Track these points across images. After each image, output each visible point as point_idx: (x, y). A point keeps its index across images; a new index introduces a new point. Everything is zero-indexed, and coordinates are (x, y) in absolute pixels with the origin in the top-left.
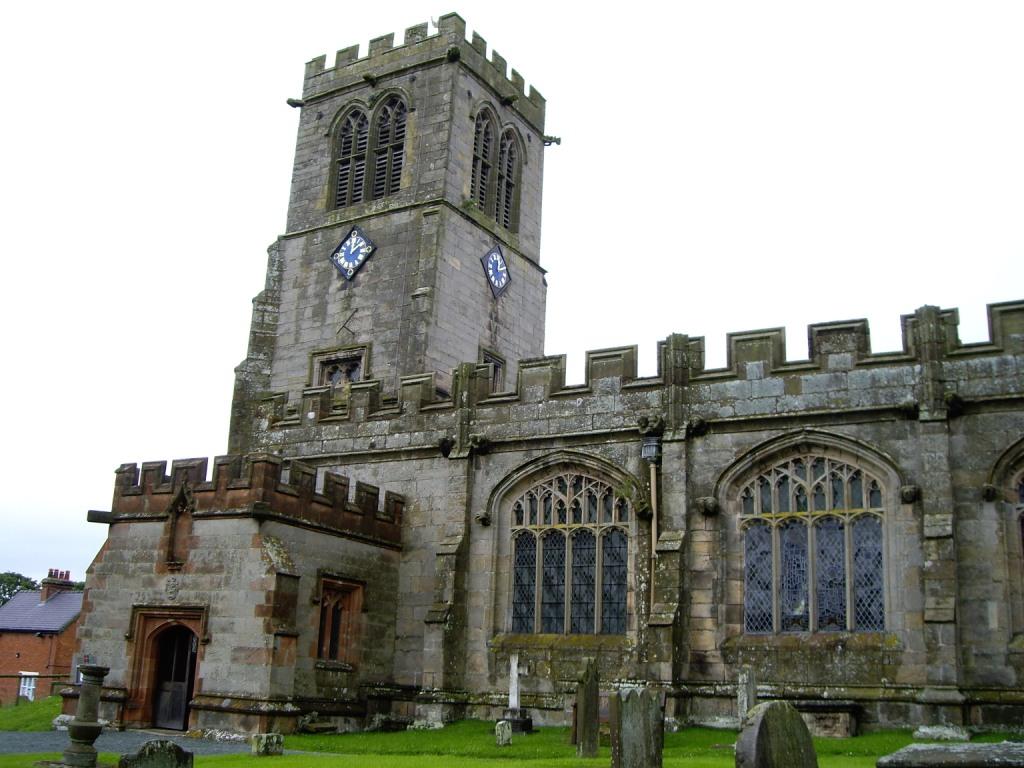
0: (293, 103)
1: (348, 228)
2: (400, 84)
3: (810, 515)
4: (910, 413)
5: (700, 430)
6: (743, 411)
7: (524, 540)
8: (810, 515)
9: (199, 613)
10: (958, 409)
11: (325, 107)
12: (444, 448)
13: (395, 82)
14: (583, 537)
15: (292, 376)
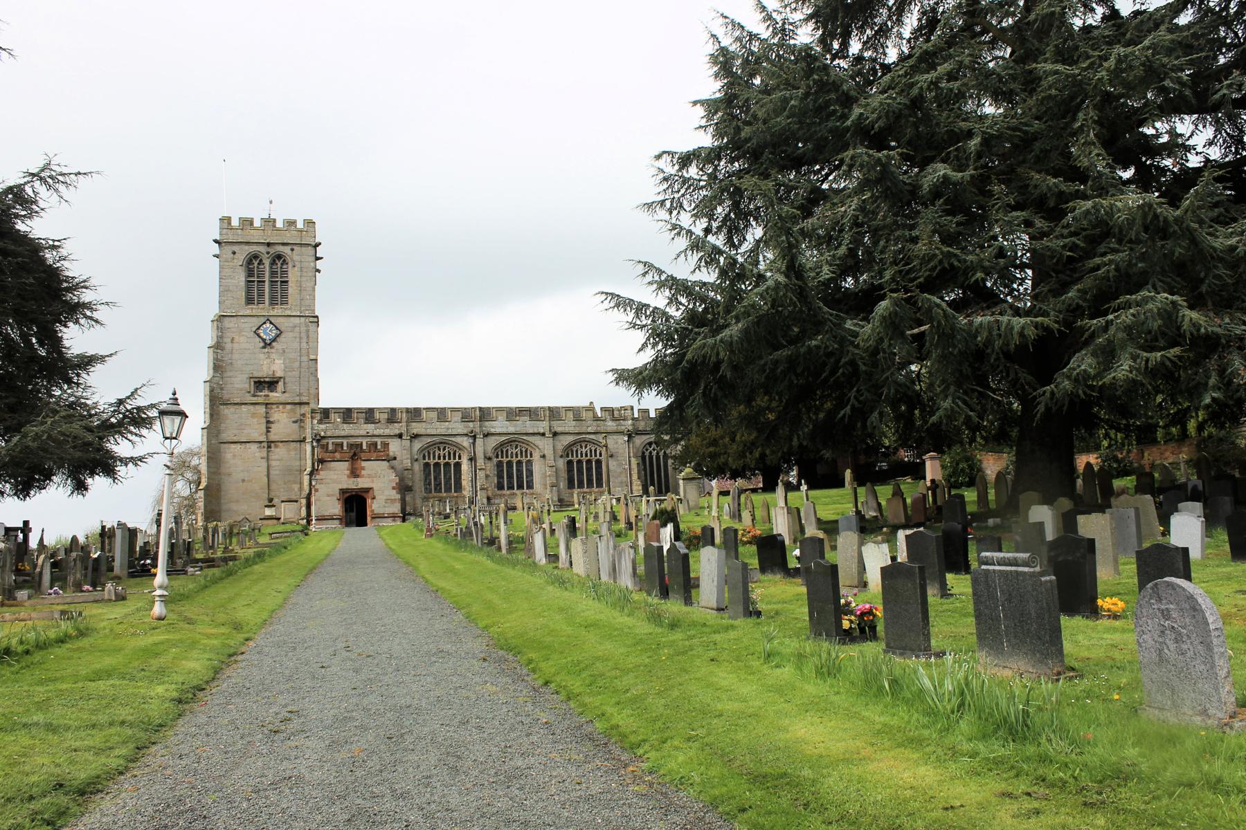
0: (216, 241)
1: (263, 320)
2: (287, 250)
3: (515, 460)
4: (543, 434)
5: (486, 435)
6: (498, 430)
7: (427, 465)
8: (515, 460)
9: (368, 490)
10: (555, 434)
11: (236, 248)
12: (400, 436)
13: (280, 248)
14: (447, 465)
15: (239, 384)
